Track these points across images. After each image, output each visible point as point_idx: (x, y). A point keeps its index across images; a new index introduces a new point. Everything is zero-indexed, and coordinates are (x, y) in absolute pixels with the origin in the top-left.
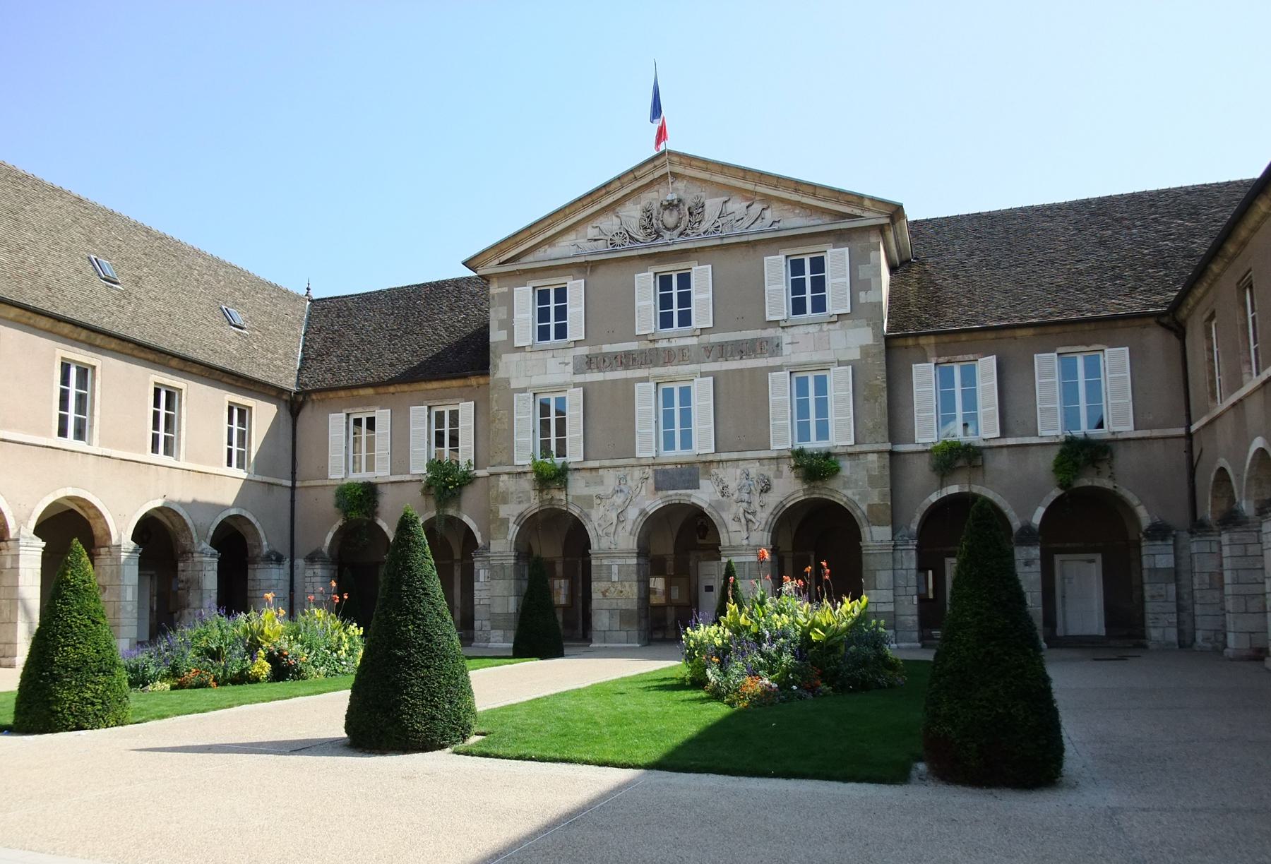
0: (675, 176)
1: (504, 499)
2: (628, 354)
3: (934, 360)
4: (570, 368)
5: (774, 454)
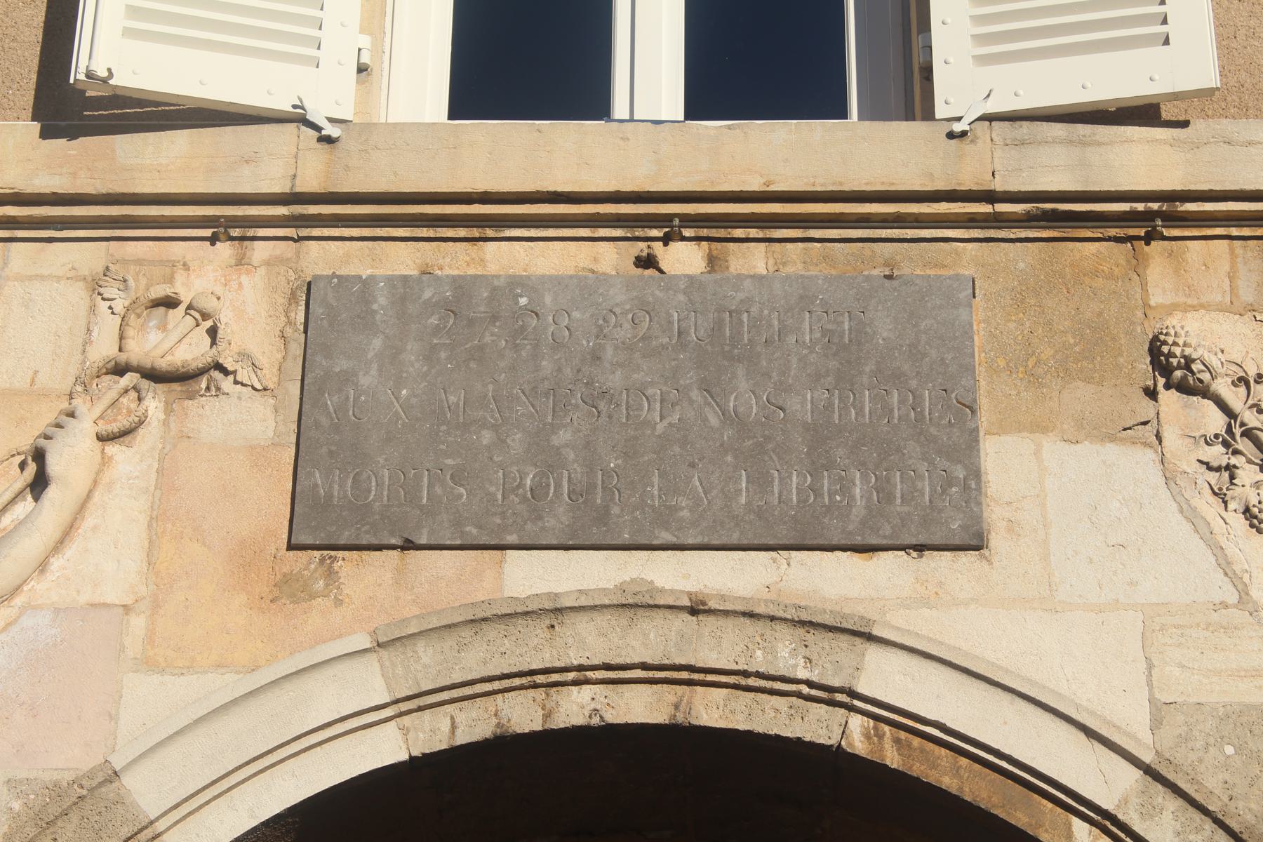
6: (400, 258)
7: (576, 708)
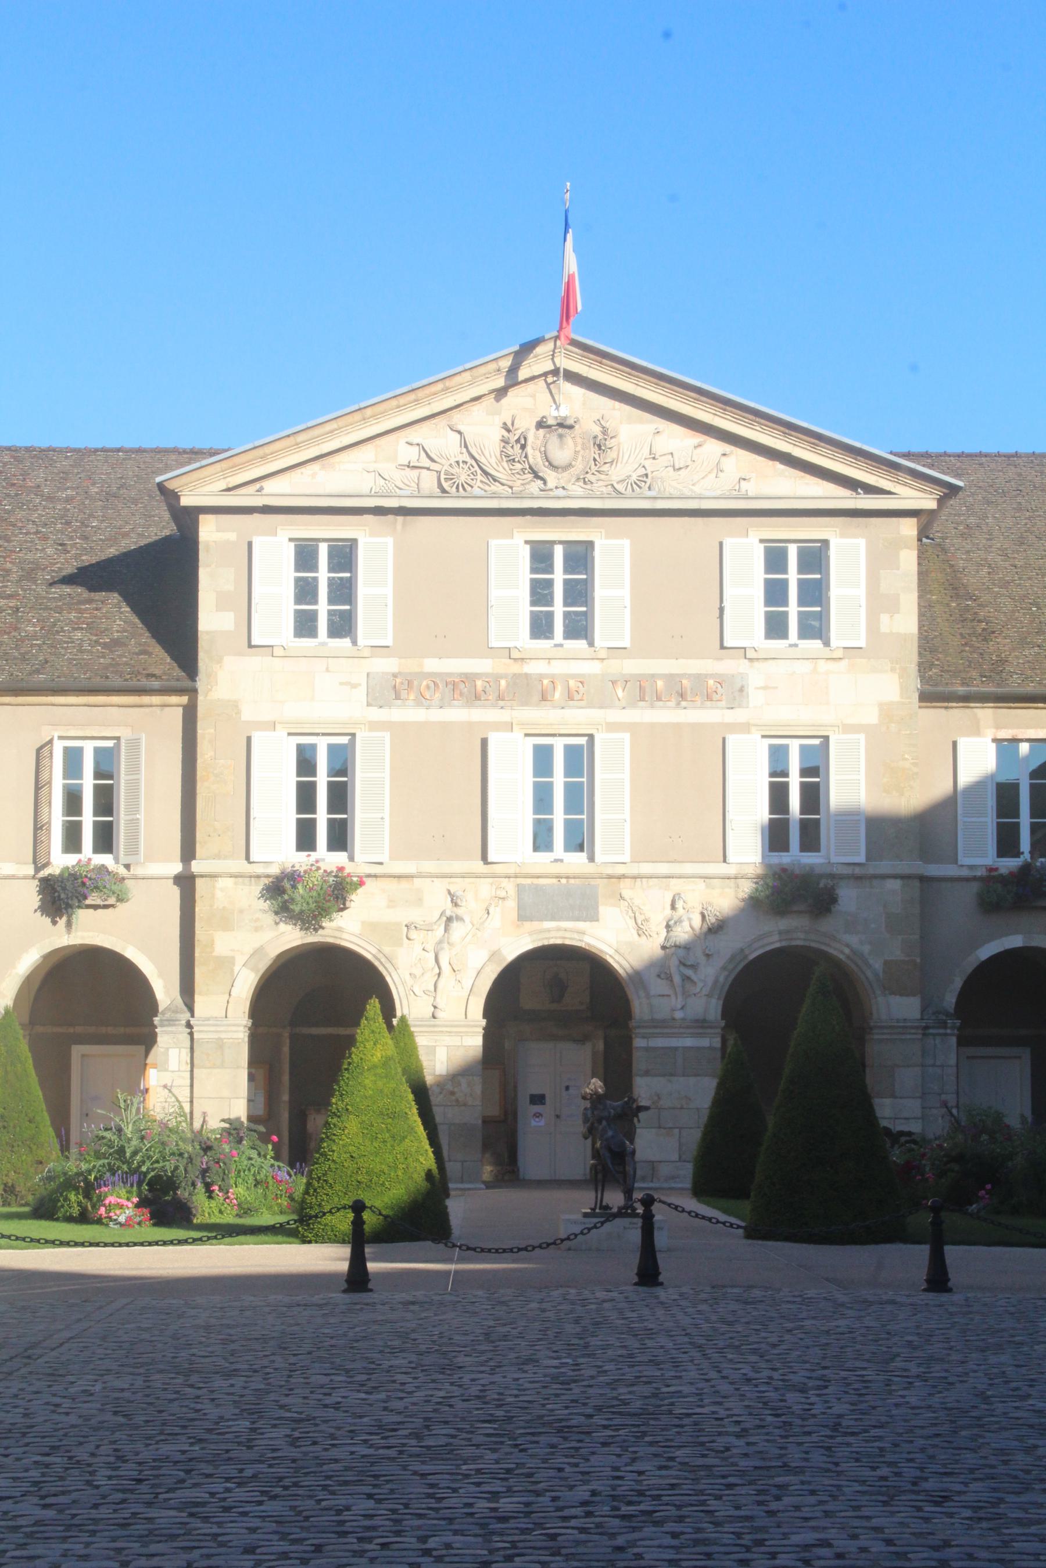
0: (573, 377)
1: (225, 921)
2: (469, 678)
3: (990, 733)
4: (361, 694)
5: (732, 870)
6: (529, 881)
7: (552, 942)
